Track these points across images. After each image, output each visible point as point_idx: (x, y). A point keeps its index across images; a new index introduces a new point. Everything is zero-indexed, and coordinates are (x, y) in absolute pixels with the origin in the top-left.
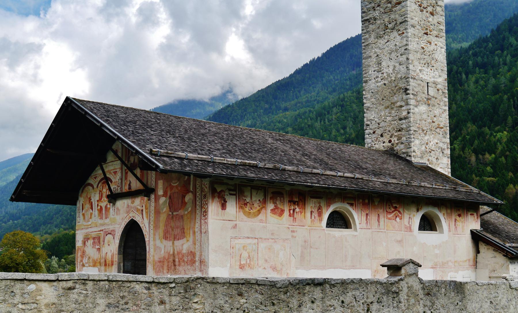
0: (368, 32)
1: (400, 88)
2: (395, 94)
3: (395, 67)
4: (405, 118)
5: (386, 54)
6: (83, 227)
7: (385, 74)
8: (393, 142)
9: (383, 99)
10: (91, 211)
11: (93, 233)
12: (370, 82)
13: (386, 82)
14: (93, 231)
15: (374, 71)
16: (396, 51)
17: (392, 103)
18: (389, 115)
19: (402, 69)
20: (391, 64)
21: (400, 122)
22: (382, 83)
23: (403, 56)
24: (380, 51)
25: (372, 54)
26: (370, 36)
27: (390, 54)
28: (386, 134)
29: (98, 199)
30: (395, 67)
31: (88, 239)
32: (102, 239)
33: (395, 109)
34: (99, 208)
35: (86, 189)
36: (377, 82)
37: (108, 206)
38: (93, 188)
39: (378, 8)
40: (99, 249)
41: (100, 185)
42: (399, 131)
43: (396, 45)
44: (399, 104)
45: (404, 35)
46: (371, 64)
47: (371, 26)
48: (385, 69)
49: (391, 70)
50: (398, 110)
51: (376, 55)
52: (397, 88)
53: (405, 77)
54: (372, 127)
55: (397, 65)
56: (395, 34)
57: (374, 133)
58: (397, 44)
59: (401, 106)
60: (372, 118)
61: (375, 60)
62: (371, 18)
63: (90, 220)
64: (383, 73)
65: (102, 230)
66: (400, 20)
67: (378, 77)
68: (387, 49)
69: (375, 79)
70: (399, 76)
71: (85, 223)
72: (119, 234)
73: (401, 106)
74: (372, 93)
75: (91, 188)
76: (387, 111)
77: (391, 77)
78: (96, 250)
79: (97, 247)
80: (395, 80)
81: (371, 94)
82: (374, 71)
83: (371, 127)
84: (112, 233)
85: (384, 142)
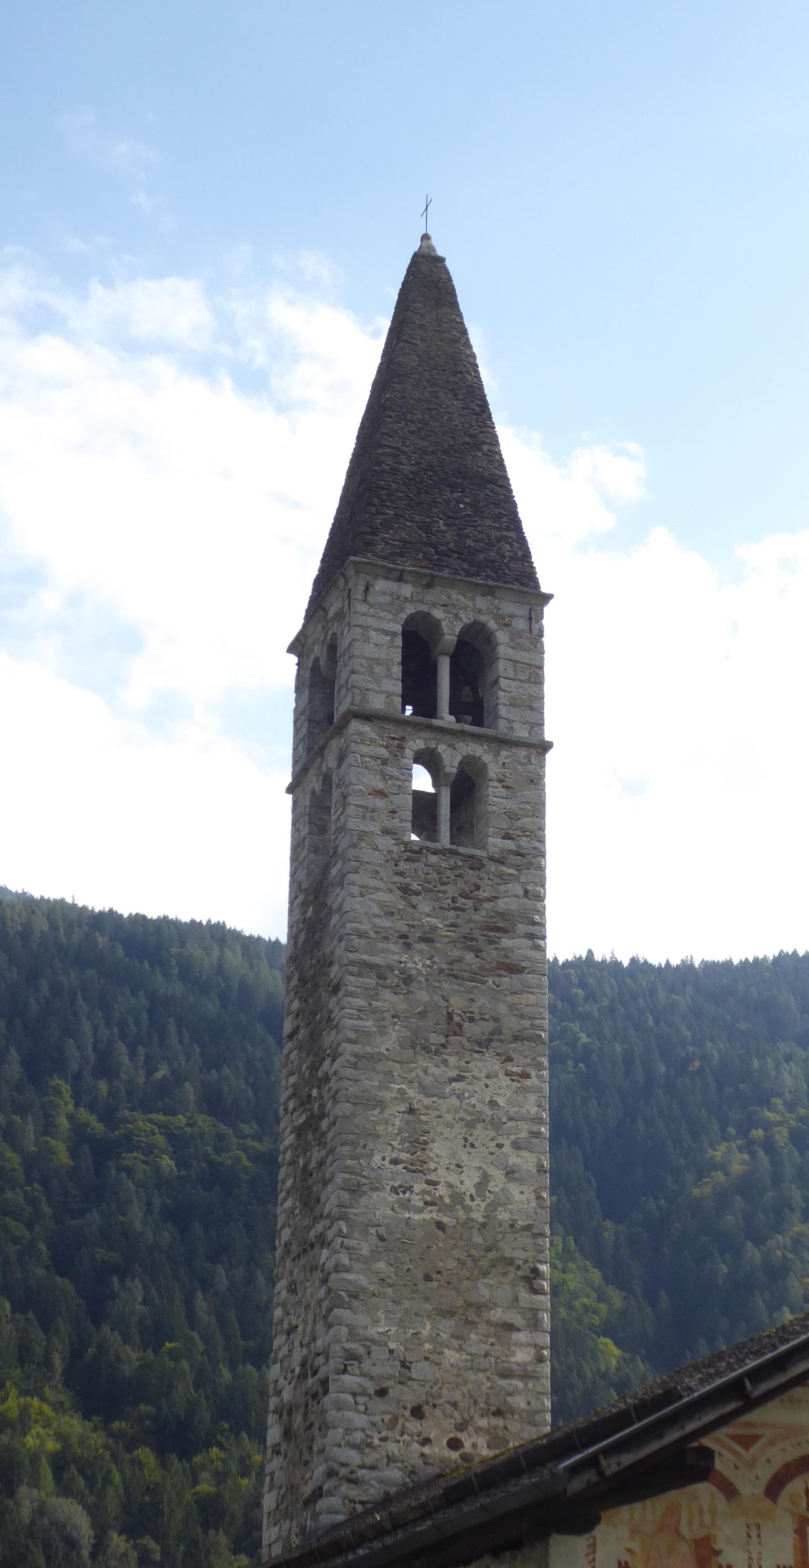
0: (375, 1011)
1: (510, 1262)
2: (486, 1274)
3: (486, 1178)
4: (525, 1376)
5: (449, 1117)
7: (442, 1190)
8: (467, 1447)
9: (428, 1278)
12: (375, 1195)
13: (445, 1220)
15: (395, 1162)
16: (496, 1125)
17: (469, 1305)
18: (455, 1343)
19: (517, 1197)
20: (472, 1162)
21: (504, 1383)
22: (426, 1216)
23: (523, 1153)
24: (427, 1101)
25: (388, 1095)
26: (382, 1031)
27: (470, 1125)
28: (438, 1412)
30: (486, 1178)
33: (483, 1328)
36: (406, 1205)
39: (423, 946)
42: (498, 1413)
43: (493, 1104)
44: (497, 1315)
45: (528, 1083)
46: (380, 1128)
47: (387, 994)
48: (441, 1172)
49: (468, 1183)
50: (498, 1337)
51: (403, 1108)
52: (492, 1255)
53: (527, 1228)
54: (376, 1371)
55: (497, 1174)
56: (488, 1063)
57: (382, 1393)
58: (501, 1102)
59: (510, 1327)
60: (373, 1332)
61: (397, 1122)
62: (391, 968)
64: (434, 1184)
66: (511, 1024)
67: (410, 1189)
68: (454, 1101)
69: (394, 1190)
70: (503, 1215)
73: (510, 1327)
74: (381, 1238)
76: (447, 1326)
77: (468, 1209)
80: (484, 1225)
81: (376, 1240)
82: (395, 1162)
83: (366, 1365)
85: (426, 1441)
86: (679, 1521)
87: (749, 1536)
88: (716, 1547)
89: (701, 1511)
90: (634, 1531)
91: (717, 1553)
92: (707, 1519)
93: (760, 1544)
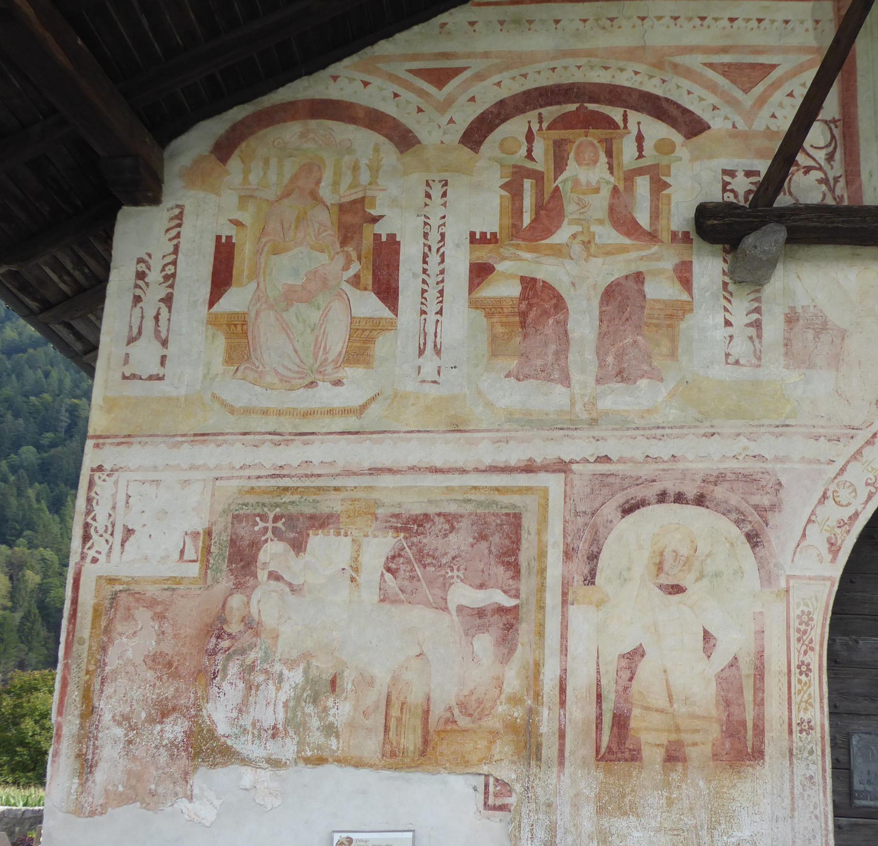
6: (212, 420)
10: (369, 305)
11: (387, 481)
14: (420, 463)
29: (490, 221)
31: (298, 529)
32: (549, 542)
34: (504, 288)
35: (290, 132)
37: (661, 289)
38: (404, 139)
40: (507, 621)
41: (514, 128)
63: (350, 373)
65: (562, 467)
71: (239, 392)
72: (832, 513)
75: (363, 140)
78: (449, 622)
79: (464, 595)
84: (719, 492)
86: (318, 182)
87: (428, 196)
88: (374, 212)
89: (355, 168)
90: (244, 200)
91: (375, 220)
92: (365, 177)
93: (444, 205)
